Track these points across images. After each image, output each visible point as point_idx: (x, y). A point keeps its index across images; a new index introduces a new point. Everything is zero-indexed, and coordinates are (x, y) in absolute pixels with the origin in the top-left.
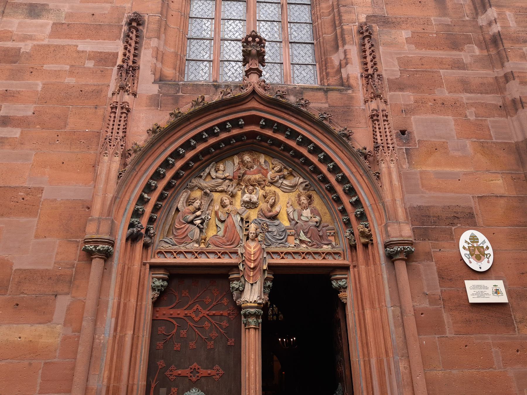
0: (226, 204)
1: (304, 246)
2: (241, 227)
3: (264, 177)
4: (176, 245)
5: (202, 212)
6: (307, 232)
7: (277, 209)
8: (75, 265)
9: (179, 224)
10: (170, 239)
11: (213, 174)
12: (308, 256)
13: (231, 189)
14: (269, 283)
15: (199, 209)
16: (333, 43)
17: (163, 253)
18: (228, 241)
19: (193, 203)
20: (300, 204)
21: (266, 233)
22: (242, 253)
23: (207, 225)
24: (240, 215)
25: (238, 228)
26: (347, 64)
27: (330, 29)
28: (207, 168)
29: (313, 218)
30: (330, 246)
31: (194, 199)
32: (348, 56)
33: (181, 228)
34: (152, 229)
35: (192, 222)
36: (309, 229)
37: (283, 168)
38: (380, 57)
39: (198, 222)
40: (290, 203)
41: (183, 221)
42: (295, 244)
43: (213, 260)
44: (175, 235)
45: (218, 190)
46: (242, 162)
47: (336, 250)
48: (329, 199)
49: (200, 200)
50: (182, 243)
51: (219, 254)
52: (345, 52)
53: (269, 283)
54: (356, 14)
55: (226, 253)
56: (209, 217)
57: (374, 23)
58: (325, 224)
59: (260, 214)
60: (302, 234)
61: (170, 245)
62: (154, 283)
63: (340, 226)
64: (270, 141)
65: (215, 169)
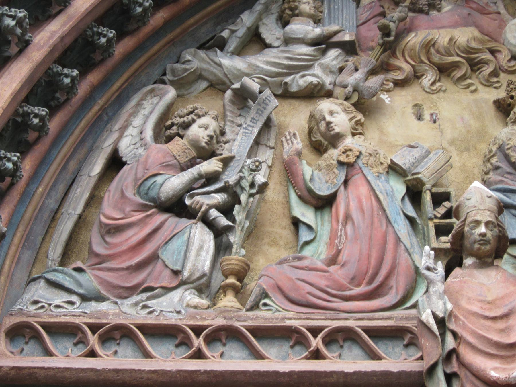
0: (337, 130)
3: (486, 37)
4: (100, 298)
9: (123, 211)
10: (74, 273)
17: (37, 337)
19: (186, 126)
22: (441, 315)
31: (191, 113)
33: (129, 226)
41: (139, 200)
44: (97, 255)
45: (294, 89)
49: (216, 118)
50: (132, 290)
59: (497, 168)
61: (74, 298)
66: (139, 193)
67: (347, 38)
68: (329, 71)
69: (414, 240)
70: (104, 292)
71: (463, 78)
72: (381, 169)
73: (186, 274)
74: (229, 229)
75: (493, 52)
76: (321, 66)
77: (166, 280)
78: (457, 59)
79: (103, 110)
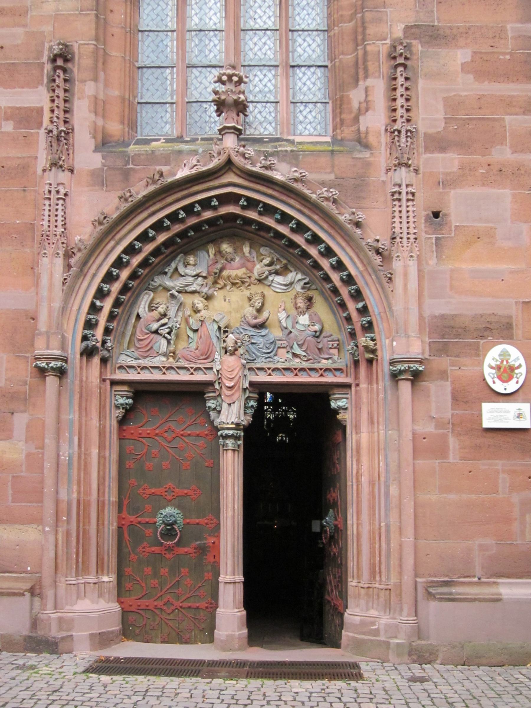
0: (199, 309)
1: (297, 360)
2: (218, 337)
3: (248, 271)
4: (139, 359)
5: (169, 319)
6: (303, 344)
7: (265, 315)
8: (28, 383)
11: (181, 270)
12: (302, 373)
13: (205, 290)
14: (252, 403)
15: (164, 315)
16: (353, 71)
17: (124, 368)
18: (202, 355)
19: (157, 308)
20: (296, 308)
21: (250, 346)
23: (177, 336)
24: (217, 322)
25: (215, 340)
26: (367, 110)
27: (350, 46)
28: (173, 262)
29: (310, 327)
30: (330, 361)
32: (369, 98)
34: (109, 341)
35: (156, 332)
36: (304, 341)
37: (275, 259)
38: (418, 98)
39: (164, 331)
40: (283, 308)
42: (286, 359)
43: (184, 376)
45: (188, 291)
46: (219, 252)
47: (336, 366)
48: (333, 302)
49: (166, 304)
50: (147, 357)
51: (192, 370)
52: (367, 90)
53: (252, 403)
54: (389, 24)
55: (199, 369)
56: (178, 326)
57: (415, 39)
58: (328, 334)
60: (295, 346)
61: (133, 359)
62: (117, 400)
63: (344, 337)
64: (255, 226)
65: (184, 263)
66: (146, 328)
67: (204, 275)
68: (198, 285)
69: (218, 343)
70: (140, 358)
71: (239, 287)
72: (211, 322)
73: (160, 353)
74: (170, 339)
75: (250, 277)
76: (196, 284)
77: (155, 355)
78: (237, 281)
79: (133, 301)
